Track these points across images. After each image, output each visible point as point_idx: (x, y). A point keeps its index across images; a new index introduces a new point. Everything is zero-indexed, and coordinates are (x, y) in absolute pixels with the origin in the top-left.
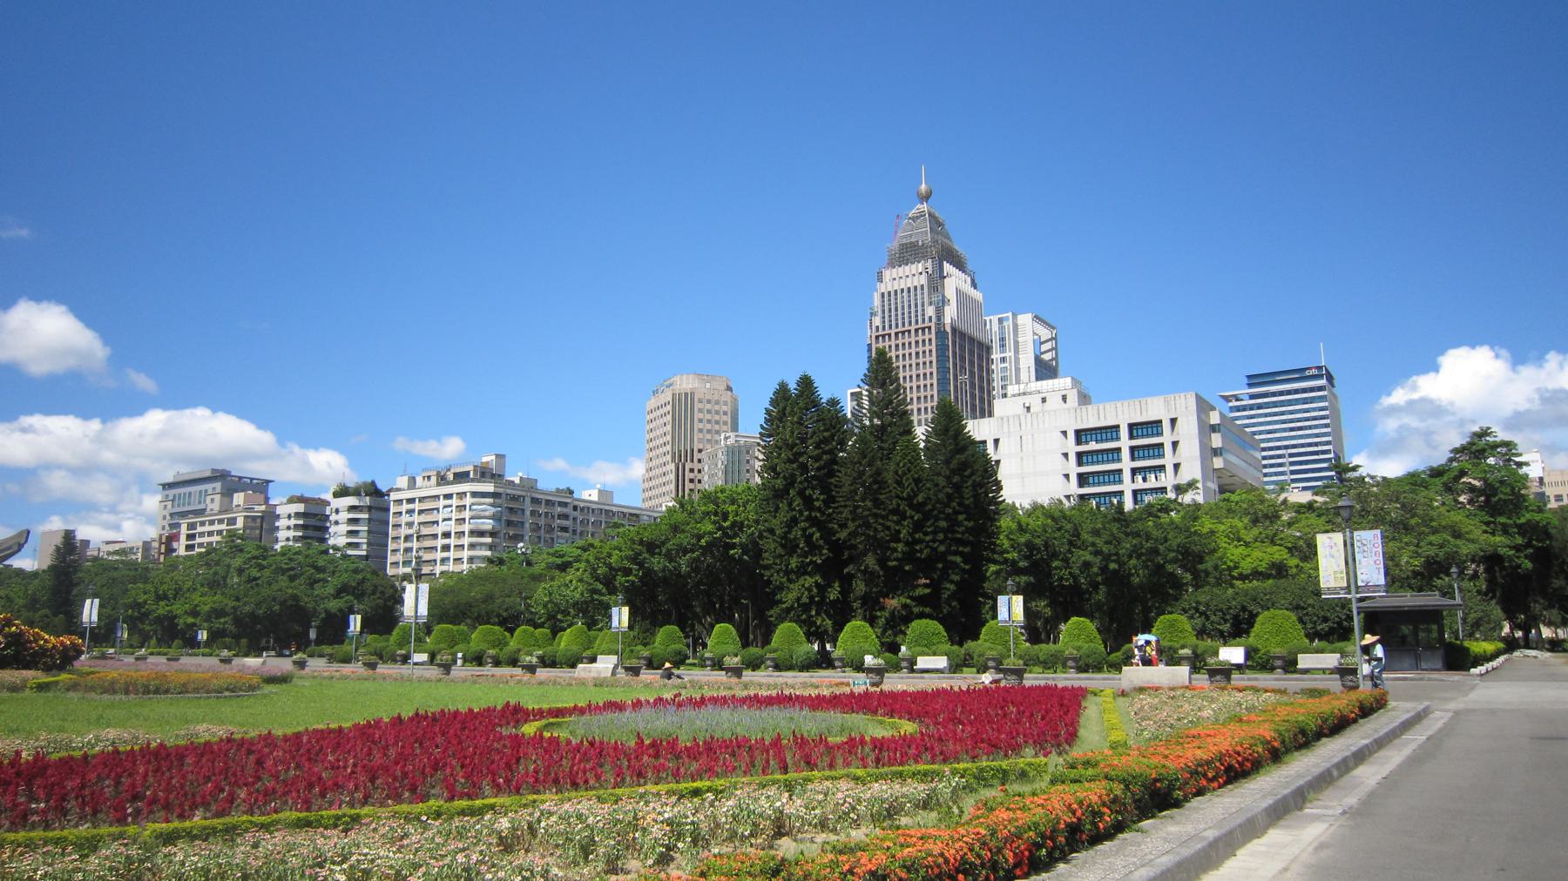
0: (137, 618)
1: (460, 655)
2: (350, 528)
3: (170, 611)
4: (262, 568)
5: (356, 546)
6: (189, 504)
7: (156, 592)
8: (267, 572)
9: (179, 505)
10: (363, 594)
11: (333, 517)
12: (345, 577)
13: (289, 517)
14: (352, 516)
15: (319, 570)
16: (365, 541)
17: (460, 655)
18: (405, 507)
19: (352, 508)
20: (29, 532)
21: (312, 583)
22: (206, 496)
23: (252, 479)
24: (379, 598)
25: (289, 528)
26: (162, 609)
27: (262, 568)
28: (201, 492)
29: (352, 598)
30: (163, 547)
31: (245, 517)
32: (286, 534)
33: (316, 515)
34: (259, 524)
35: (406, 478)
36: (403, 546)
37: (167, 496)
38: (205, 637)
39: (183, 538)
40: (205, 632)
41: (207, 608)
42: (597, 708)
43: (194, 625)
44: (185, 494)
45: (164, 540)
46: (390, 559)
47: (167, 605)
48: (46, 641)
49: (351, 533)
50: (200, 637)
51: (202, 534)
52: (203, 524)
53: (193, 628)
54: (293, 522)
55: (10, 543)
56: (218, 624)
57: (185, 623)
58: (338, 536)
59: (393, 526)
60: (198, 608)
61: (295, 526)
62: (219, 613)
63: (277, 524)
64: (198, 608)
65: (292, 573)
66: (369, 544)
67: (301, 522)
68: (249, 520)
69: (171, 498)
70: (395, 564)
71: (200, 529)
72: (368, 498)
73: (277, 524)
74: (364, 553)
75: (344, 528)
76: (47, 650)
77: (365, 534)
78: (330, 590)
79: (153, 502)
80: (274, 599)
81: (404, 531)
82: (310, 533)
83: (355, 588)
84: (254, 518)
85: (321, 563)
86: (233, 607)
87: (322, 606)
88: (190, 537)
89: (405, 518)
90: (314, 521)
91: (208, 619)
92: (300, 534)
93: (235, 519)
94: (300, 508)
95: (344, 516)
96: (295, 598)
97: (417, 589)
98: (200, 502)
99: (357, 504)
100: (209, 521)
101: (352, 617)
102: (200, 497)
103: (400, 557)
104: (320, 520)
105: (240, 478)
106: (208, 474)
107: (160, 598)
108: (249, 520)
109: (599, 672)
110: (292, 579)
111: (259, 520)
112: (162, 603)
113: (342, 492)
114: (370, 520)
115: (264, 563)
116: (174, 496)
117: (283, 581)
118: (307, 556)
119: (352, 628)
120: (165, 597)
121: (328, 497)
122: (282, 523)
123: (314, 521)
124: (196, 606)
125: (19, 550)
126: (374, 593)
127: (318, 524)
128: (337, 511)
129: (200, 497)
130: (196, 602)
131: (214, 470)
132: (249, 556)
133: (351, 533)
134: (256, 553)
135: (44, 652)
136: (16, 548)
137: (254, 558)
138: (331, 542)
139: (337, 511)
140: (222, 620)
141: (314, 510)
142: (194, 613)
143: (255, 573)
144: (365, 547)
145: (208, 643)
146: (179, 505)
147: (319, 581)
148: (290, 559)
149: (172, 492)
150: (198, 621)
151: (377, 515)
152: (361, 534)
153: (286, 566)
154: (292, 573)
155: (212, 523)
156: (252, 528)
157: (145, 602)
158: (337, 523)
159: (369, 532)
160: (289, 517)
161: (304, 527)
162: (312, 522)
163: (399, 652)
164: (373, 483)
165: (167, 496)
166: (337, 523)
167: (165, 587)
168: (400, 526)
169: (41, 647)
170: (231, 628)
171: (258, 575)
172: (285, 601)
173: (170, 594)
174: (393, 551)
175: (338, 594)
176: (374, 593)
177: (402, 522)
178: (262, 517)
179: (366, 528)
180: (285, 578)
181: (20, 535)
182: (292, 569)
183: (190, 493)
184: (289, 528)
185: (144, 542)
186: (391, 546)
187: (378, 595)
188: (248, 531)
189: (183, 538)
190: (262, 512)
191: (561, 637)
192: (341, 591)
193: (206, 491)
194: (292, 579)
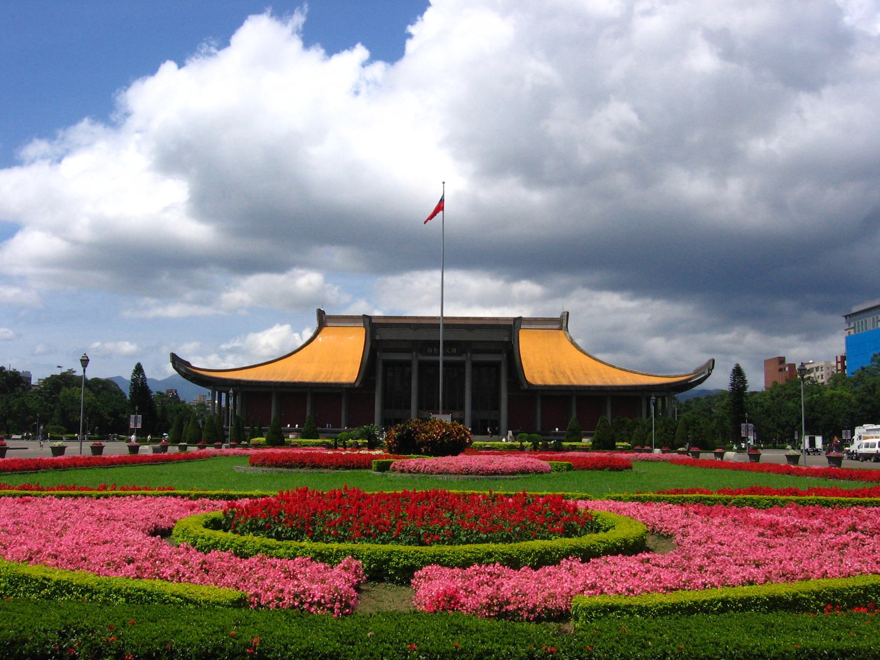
20: (714, 361)
30: (839, 365)
45: (839, 360)
125: (709, 374)
136: (707, 373)
181: (708, 363)
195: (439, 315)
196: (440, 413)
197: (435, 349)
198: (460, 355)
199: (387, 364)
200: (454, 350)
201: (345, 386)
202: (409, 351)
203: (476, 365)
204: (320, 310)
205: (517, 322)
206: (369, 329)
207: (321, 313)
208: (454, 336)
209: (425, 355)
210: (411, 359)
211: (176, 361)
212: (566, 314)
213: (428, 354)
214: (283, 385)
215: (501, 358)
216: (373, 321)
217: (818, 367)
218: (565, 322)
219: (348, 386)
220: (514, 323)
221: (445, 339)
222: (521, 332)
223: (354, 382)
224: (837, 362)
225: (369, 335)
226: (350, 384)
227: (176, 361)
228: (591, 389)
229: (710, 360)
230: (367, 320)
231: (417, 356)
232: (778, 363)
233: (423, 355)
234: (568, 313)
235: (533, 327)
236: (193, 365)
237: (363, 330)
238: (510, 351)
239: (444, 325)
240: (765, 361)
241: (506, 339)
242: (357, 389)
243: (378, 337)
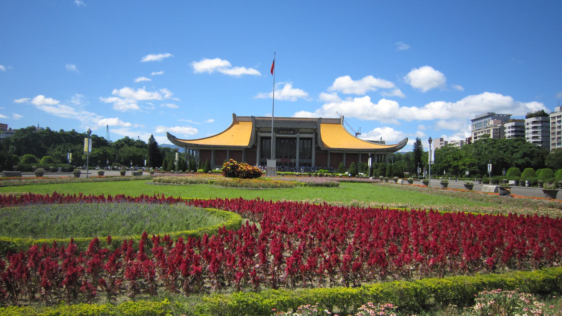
0: (448, 167)
1: (527, 182)
2: (534, 130)
3: (458, 164)
4: (494, 147)
5: (537, 137)
6: (481, 126)
7: (453, 157)
8: (495, 149)
9: (479, 127)
10: (534, 157)
11: (526, 127)
12: (525, 150)
13: (509, 128)
14: (534, 125)
15: (515, 147)
16: (541, 135)
17: (527, 182)
18: (557, 120)
19: (534, 122)
20: (408, 139)
21: (513, 153)
22: (486, 123)
23: (503, 115)
24: (540, 158)
25: (509, 132)
26: (455, 163)
27: (494, 147)
28: (485, 121)
29: (528, 158)
30: (467, 142)
31: (493, 129)
32: (508, 133)
33: (521, 126)
34: (499, 132)
35: (559, 107)
36: (557, 136)
37: (473, 124)
38: (468, 174)
39: (473, 138)
40: (468, 172)
41: (468, 163)
42: (85, 198)
43: (465, 169)
44: (479, 123)
45: (467, 140)
46: (551, 142)
47: (457, 162)
48: (242, 168)
49: (534, 132)
50: (466, 174)
51: (479, 137)
52: (479, 133)
53: (464, 170)
54: (511, 130)
55: (403, 142)
56: (473, 169)
57: (462, 168)
58: (529, 135)
59: (552, 128)
60: (465, 163)
61: (512, 131)
62: (472, 165)
63: (505, 131)
64: (465, 163)
65: (504, 149)
66: (542, 136)
67: (514, 130)
68: (495, 130)
69: (475, 125)
70: (554, 144)
71: (478, 135)
72: (540, 118)
73: (505, 131)
74: (540, 140)
75: (531, 131)
76: (242, 171)
77: (540, 133)
78: (518, 155)
79: (470, 128)
80: (494, 159)
81: (557, 130)
82: (518, 134)
83: (529, 154)
84: (497, 129)
85: (515, 145)
86: (478, 163)
87: (514, 162)
88: (475, 138)
89: (557, 125)
90: (519, 129)
91: (469, 167)
92: (514, 134)
93: (490, 130)
94: (513, 124)
95: (531, 126)
96: (502, 159)
97: (308, 142)
98: (485, 125)
99: (536, 120)
100: (484, 131)
101: (488, 165)
102: (485, 123)
103: (555, 141)
104: (522, 128)
105: (499, 115)
106: (487, 115)
107: (455, 159)
108: (495, 130)
109: (490, 190)
110: (505, 152)
111: (498, 130)
112: (455, 161)
113: (529, 116)
114: (542, 127)
115: (494, 146)
116: (476, 124)
117: (501, 152)
118: (510, 143)
119: (488, 170)
120: (455, 159)
121: (524, 118)
122: (507, 130)
123: (519, 129)
124: (465, 162)
125: (406, 145)
126: (538, 156)
127: (521, 130)
128: (528, 124)
129: (485, 123)
130: (465, 161)
131: (488, 113)
132: (489, 143)
133: (534, 132)
134: (492, 142)
135: (241, 172)
137: (492, 144)
138: (526, 136)
139: (528, 124)
140: (474, 167)
141: (519, 124)
142: (464, 165)
143: (491, 149)
144: (540, 138)
145: (469, 176)
146: (478, 127)
147: (516, 152)
148: (504, 144)
149: (475, 123)
150: (466, 167)
151: (545, 124)
152: (538, 132)
153: (502, 147)
154: (504, 149)
155: (482, 132)
156: (496, 133)
157: (450, 161)
158: (528, 129)
159: (542, 131)
160: (509, 128)
161: (515, 131)
162: (518, 129)
163: (503, 180)
164: (543, 111)
165: (473, 124)
166: (528, 129)
167: (456, 156)
168: (555, 128)
169: (240, 170)
170: (477, 170)
171: (493, 150)
172: (498, 160)
173: (458, 158)
174: (552, 139)
175: (523, 157)
176: (538, 156)
177: (555, 126)
178: (500, 129)
179: (541, 130)
180: (502, 151)
181: (405, 140)
182: (504, 148)
183: (481, 122)
184: (509, 132)
185: (461, 141)
186: (551, 137)
187: (540, 157)
188: (495, 134)
189: (473, 138)
190: (499, 127)
191: (540, 171)
192: (525, 155)
193: (486, 121)
194: (505, 152)
195: (271, 116)
196: (243, 160)
198: (295, 134)
199: (263, 138)
200: (292, 132)
201: (244, 147)
203: (301, 139)
204: (233, 114)
207: (234, 115)
208: (279, 126)
211: (170, 137)
214: (216, 146)
216: (256, 119)
219: (245, 148)
221: (275, 127)
222: (321, 124)
223: (247, 145)
224: (466, 141)
225: (254, 125)
226: (246, 146)
227: (170, 137)
228: (342, 150)
229: (406, 139)
230: (253, 119)
231: (275, 135)
233: (278, 134)
234: (343, 117)
235: (261, 119)
236: (177, 137)
237: (252, 123)
238: (316, 133)
239: (274, 120)
241: (315, 128)
242: (249, 149)
243: (258, 126)
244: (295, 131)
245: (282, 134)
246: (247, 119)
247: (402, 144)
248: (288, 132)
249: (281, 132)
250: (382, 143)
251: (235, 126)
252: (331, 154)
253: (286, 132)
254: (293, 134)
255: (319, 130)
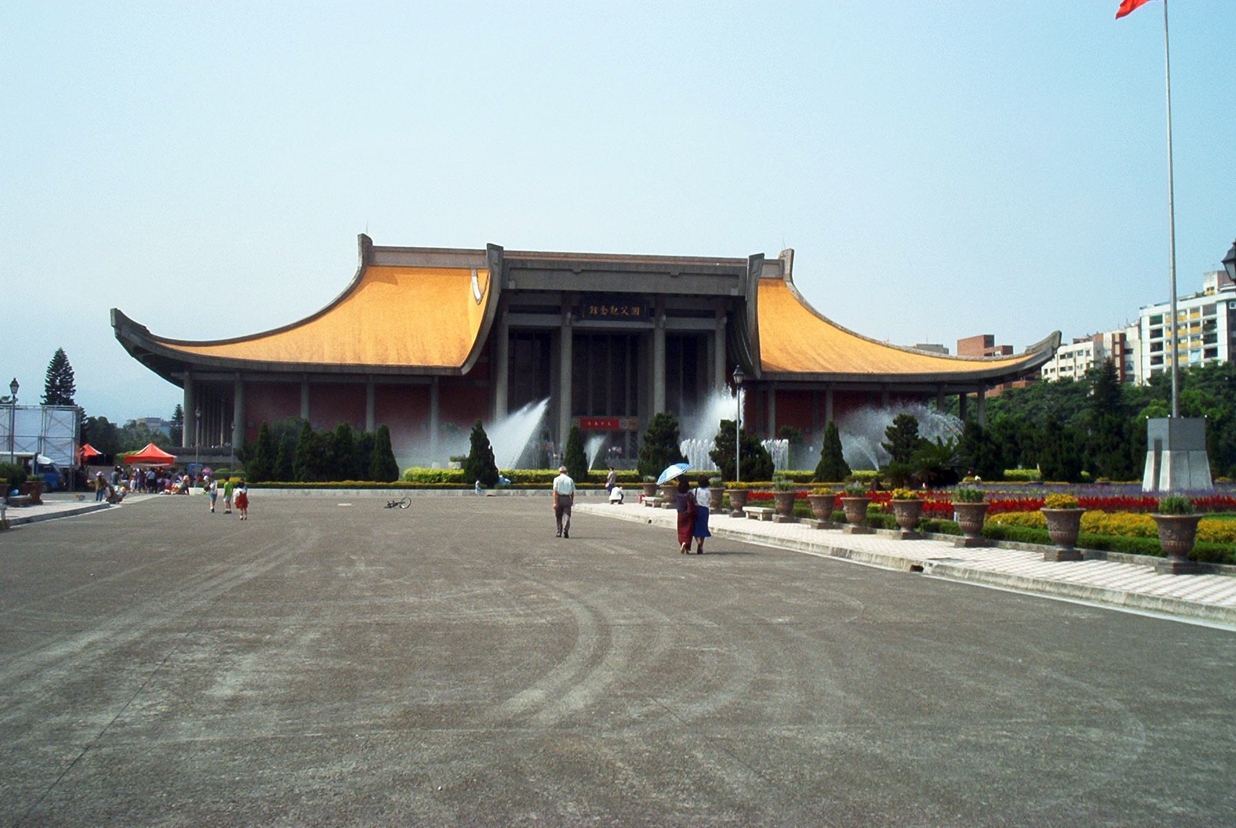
20: (1061, 334)
136: (1050, 355)
197: (603, 308)
199: (517, 335)
200: (636, 311)
202: (556, 310)
205: (756, 262)
206: (497, 269)
207: (365, 241)
209: (585, 319)
210: (559, 325)
212: (790, 253)
213: (593, 317)
215: (716, 325)
217: (1082, 351)
218: (787, 267)
219: (449, 373)
220: (751, 265)
224: (1114, 343)
226: (454, 369)
232: (982, 346)
234: (793, 251)
240: (958, 341)
243: (512, 286)
244: (650, 304)
245: (599, 317)
246: (418, 260)
247: (1045, 353)
248: (620, 311)
249: (594, 310)
250: (940, 350)
251: (371, 290)
252: (780, 394)
253: (614, 310)
254: (641, 318)
255: (750, 306)
